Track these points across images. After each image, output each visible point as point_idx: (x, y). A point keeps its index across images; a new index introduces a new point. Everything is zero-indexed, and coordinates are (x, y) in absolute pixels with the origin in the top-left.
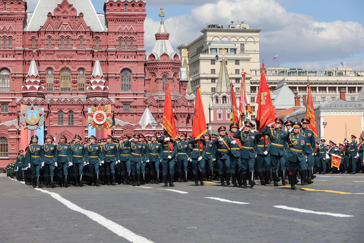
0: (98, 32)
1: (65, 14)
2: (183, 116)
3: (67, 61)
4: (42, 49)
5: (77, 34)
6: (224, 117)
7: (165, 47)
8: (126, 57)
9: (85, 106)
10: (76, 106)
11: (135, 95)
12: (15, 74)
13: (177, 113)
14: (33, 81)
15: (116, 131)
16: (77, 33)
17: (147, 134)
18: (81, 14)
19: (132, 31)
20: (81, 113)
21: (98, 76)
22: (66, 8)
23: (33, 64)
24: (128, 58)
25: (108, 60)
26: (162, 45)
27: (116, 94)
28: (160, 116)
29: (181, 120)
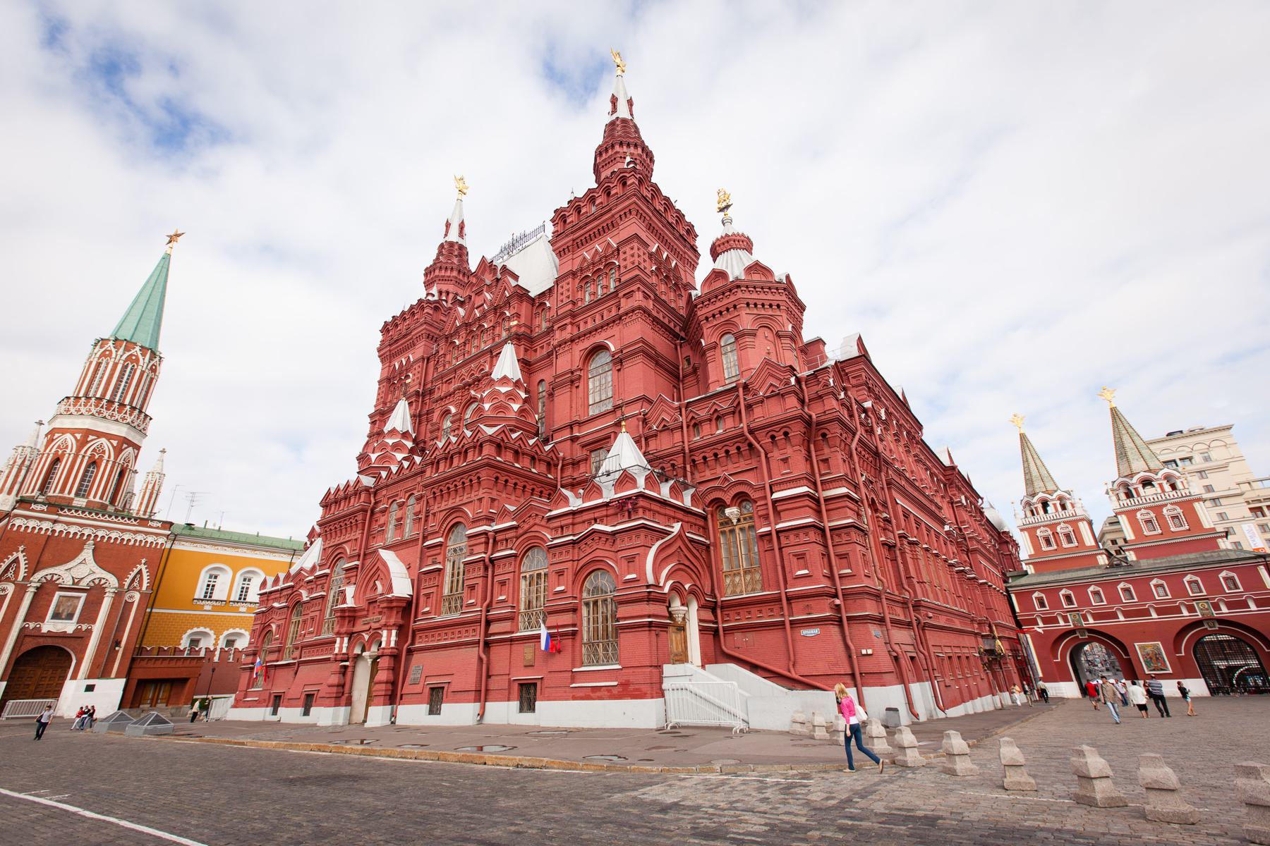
2: (780, 436)
6: (1164, 526)
15: (497, 532)
17: (589, 522)
27: (571, 426)
28: (699, 459)
29: (776, 455)
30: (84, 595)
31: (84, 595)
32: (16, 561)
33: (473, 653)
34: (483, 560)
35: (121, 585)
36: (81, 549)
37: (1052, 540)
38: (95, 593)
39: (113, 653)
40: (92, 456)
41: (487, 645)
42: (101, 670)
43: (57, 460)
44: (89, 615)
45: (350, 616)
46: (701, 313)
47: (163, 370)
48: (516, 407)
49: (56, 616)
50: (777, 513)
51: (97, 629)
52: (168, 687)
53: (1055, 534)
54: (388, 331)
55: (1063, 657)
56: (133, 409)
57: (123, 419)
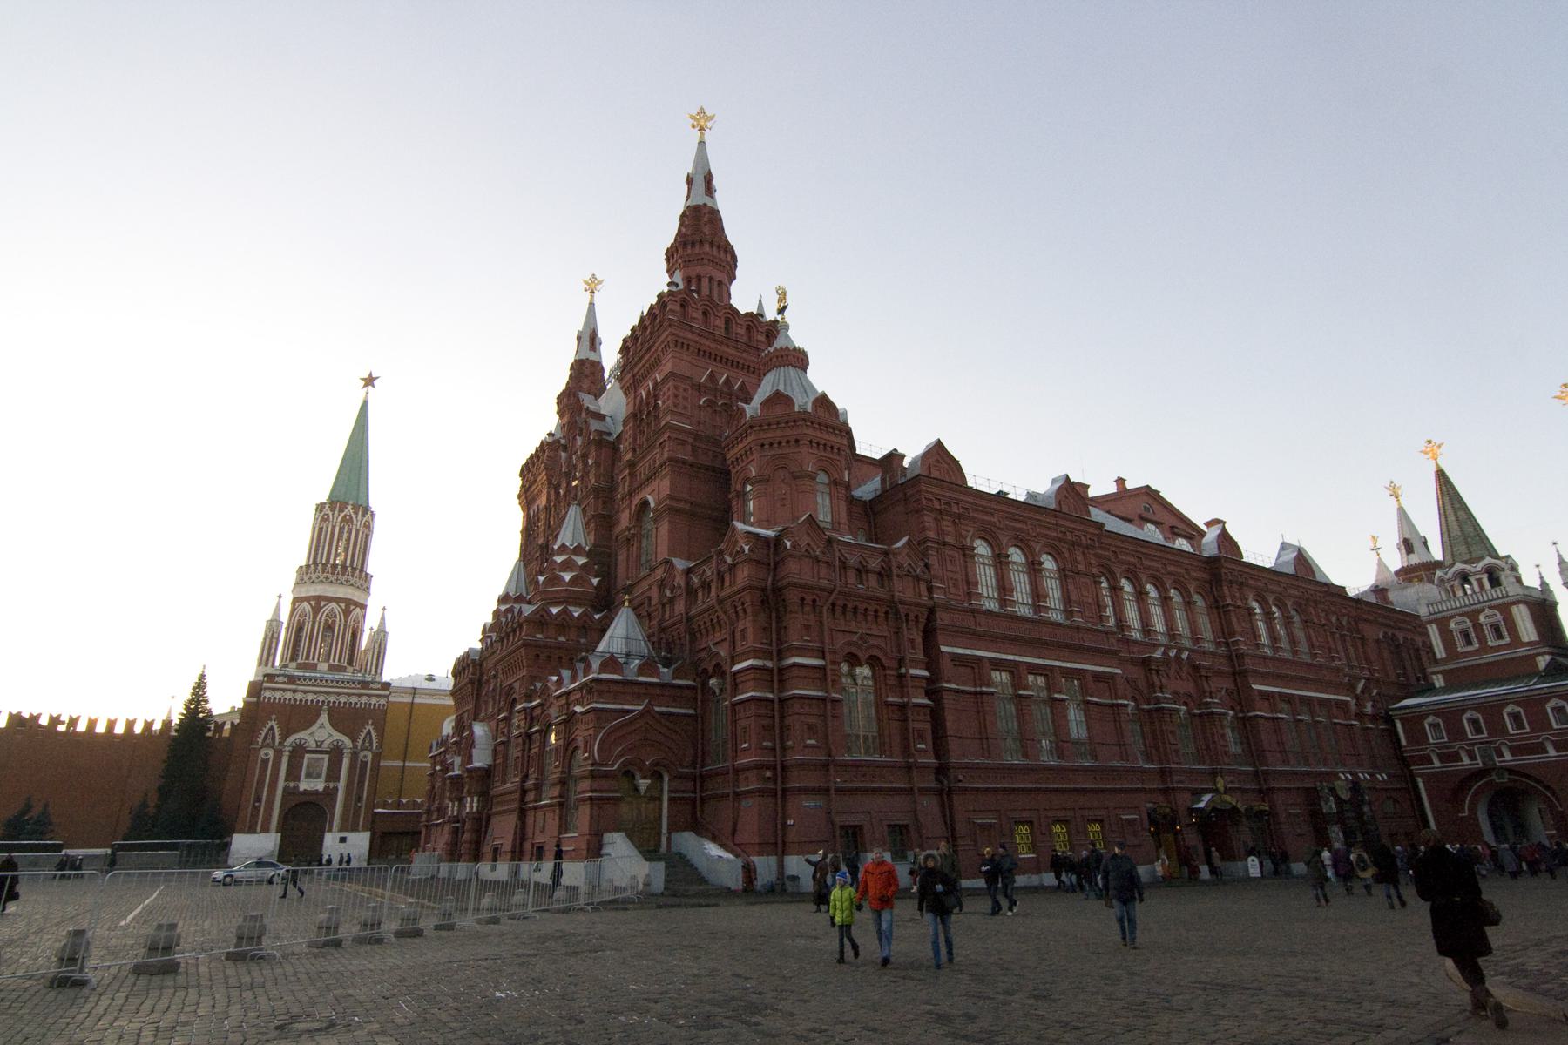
30: (326, 757)
31: (326, 757)
32: (272, 728)
33: (512, 819)
35: (355, 746)
37: (1473, 635)
38: (336, 753)
39: (357, 810)
41: (522, 813)
42: (350, 825)
43: (300, 629)
44: (333, 775)
47: (379, 526)
48: (567, 577)
49: (309, 775)
51: (342, 784)
53: (1477, 626)
55: (1473, 810)
56: (354, 569)
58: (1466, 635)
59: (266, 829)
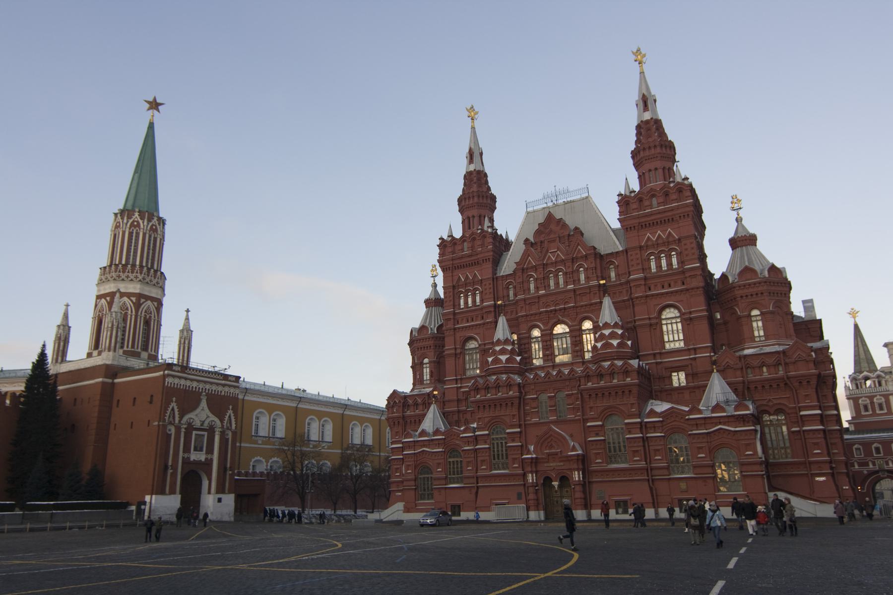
0: (612, 254)
1: (552, 236)
3: (560, 310)
4: (519, 297)
5: (573, 262)
7: (750, 260)
8: (666, 285)
9: (583, 381)
10: (567, 383)
11: (693, 352)
12: (485, 345)
13: (788, 378)
14: (498, 348)
16: (573, 260)
17: (716, 424)
18: (576, 228)
19: (671, 239)
20: (577, 394)
21: (606, 325)
22: (553, 227)
23: (502, 321)
24: (670, 286)
25: (633, 296)
26: (742, 257)
27: (654, 355)
28: (752, 386)
30: (206, 433)
31: (206, 433)
34: (643, 438)
35: (223, 426)
36: (200, 400)
40: (145, 318)
42: (221, 490)
44: (210, 451)
45: (535, 462)
46: (738, 293)
49: (195, 449)
50: (803, 421)
52: (583, 496)
54: (445, 246)
57: (136, 277)
58: (866, 407)
59: (172, 492)
